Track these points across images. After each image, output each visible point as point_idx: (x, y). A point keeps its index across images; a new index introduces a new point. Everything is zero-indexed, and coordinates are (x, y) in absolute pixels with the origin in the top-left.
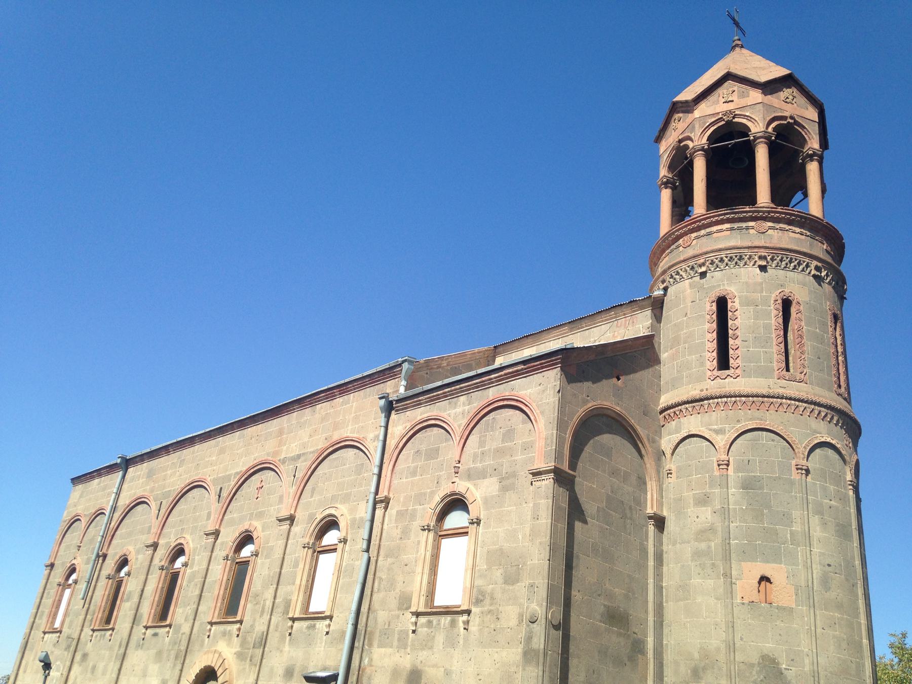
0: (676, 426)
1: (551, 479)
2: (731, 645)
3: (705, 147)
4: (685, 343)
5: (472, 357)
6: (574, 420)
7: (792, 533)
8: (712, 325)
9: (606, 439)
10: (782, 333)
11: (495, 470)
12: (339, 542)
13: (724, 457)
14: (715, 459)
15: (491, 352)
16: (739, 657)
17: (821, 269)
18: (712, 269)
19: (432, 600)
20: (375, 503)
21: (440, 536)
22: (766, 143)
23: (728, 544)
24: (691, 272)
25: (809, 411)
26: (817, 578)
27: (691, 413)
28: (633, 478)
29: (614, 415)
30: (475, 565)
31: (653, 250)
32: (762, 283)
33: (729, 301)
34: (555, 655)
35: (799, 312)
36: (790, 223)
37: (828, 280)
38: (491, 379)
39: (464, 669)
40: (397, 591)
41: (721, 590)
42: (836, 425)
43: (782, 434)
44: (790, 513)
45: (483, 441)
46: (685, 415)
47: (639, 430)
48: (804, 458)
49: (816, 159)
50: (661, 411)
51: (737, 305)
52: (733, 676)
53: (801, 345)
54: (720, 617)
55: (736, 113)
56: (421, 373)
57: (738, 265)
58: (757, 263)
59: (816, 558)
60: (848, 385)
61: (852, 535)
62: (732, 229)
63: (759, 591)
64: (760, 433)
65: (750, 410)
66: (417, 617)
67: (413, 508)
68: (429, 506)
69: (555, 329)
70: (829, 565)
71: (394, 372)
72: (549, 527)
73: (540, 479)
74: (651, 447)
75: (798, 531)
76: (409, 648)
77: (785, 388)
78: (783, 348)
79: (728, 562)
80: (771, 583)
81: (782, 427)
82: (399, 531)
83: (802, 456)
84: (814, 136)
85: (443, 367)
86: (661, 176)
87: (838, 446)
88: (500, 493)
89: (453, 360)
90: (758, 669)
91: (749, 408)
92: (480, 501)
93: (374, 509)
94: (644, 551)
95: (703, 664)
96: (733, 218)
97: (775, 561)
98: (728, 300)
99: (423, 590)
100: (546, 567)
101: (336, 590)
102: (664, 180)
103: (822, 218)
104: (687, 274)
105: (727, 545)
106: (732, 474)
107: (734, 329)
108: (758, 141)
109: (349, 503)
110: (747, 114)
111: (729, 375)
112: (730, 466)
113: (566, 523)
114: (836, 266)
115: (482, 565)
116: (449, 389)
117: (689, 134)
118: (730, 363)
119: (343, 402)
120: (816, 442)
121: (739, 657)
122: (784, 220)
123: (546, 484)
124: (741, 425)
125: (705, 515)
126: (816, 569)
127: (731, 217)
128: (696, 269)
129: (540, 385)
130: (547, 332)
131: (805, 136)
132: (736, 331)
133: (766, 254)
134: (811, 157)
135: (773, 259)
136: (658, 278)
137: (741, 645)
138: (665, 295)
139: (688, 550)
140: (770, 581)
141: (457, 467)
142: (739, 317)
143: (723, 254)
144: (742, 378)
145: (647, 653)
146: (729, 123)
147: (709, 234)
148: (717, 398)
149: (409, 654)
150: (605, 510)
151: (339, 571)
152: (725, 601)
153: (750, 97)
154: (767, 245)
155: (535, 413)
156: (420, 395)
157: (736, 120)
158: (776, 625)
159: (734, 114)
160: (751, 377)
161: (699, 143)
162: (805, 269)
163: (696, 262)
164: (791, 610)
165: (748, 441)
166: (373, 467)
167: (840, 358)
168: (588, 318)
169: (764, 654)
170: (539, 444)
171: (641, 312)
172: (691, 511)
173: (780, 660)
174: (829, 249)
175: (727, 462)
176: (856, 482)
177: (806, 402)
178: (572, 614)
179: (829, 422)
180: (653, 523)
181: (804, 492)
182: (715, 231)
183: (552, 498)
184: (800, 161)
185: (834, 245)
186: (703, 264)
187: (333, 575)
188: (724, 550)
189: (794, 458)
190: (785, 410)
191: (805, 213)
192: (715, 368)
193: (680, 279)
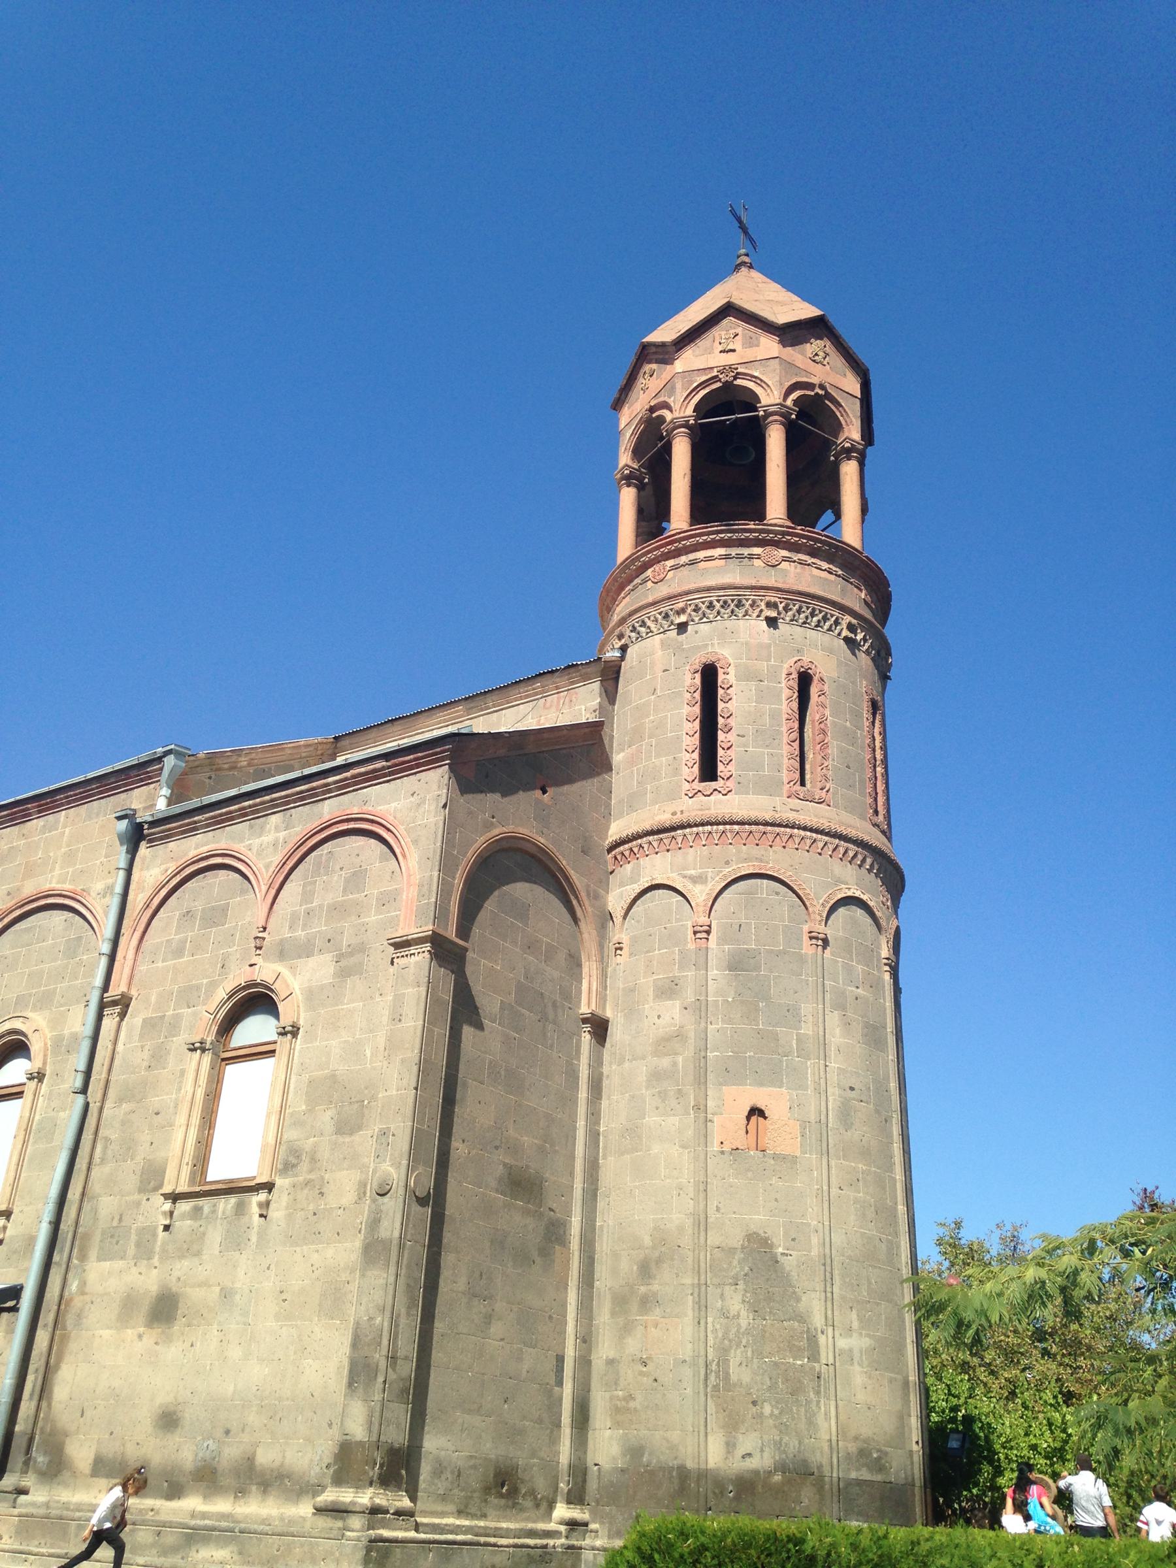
0: (632, 872)
1: (426, 953)
2: (701, 1220)
3: (690, 422)
4: (651, 738)
5: (295, 754)
6: (469, 854)
8: (694, 708)
9: (521, 890)
10: (796, 725)
11: (329, 941)
12: (28, 1079)
13: (703, 920)
14: (690, 924)
15: (328, 747)
16: (714, 1239)
17: (857, 630)
18: (696, 619)
19: (204, 1172)
20: (102, 1006)
21: (223, 1060)
22: (782, 423)
23: (704, 1057)
24: (665, 622)
25: (831, 849)
27: (657, 850)
28: (562, 956)
29: (533, 850)
30: (286, 1105)
31: (605, 585)
32: (770, 644)
33: (720, 671)
34: (419, 1248)
36: (813, 553)
37: (866, 647)
39: (256, 1285)
40: (139, 1158)
41: (690, 1132)
42: (870, 871)
43: (790, 883)
45: (310, 891)
46: (647, 853)
47: (574, 877)
49: (856, 457)
50: (610, 847)
51: (731, 678)
52: (702, 1270)
53: (824, 745)
55: (739, 370)
56: (198, 777)
58: (764, 613)
59: (833, 1077)
60: (888, 811)
61: (887, 1042)
62: (727, 557)
63: (747, 1132)
64: (759, 881)
65: (745, 844)
66: (174, 1202)
67: (176, 1012)
68: (205, 1008)
69: (442, 709)
70: (852, 1089)
71: (148, 772)
72: (419, 1033)
73: (406, 953)
74: (592, 906)
75: (807, 1035)
76: (157, 1257)
77: (798, 811)
78: (798, 749)
79: (703, 1088)
80: (765, 1118)
82: (146, 1055)
83: (819, 918)
84: (854, 420)
85: (241, 767)
86: (621, 464)
87: (871, 904)
88: (336, 980)
89: (260, 756)
90: (742, 1256)
92: (300, 998)
93: (100, 1017)
94: (573, 1075)
95: (657, 1254)
97: (772, 1083)
98: (719, 669)
99: (187, 1155)
100: (411, 1100)
101: (19, 1164)
102: (626, 472)
103: (859, 548)
104: (658, 626)
105: (702, 1060)
106: (715, 947)
107: (726, 716)
108: (771, 418)
109: (51, 1009)
110: (756, 374)
111: (715, 790)
112: (711, 934)
113: (448, 1028)
114: (878, 626)
115: (298, 1105)
116: (251, 802)
117: (666, 399)
118: (719, 771)
119: (44, 826)
120: (839, 896)
121: (714, 1239)
122: (804, 548)
123: (416, 963)
124: (730, 869)
125: (672, 1013)
126: (833, 1094)
127: (726, 538)
128: (672, 618)
129: (413, 795)
130: (426, 714)
131: (841, 418)
133: (777, 600)
134: (848, 453)
135: (786, 609)
136: (614, 629)
137: (717, 1218)
138: (622, 658)
139: (642, 1071)
140: (764, 1114)
141: (260, 938)
142: (734, 697)
143: (713, 596)
145: (570, 1243)
146: (728, 386)
147: (693, 563)
148: (696, 825)
149: (156, 1267)
151: (27, 1130)
152: (695, 1150)
153: (761, 347)
154: (780, 585)
155: (403, 843)
156: (196, 813)
157: (739, 382)
158: (771, 1185)
159: (735, 371)
161: (682, 415)
162: (833, 629)
163: (671, 607)
164: (794, 1160)
165: (740, 894)
166: (101, 943)
167: (879, 769)
168: (497, 692)
169: (749, 1232)
170: (407, 897)
172: (650, 1007)
174: (869, 599)
175: (708, 928)
176: (894, 960)
177: (828, 834)
178: (449, 1180)
179: (860, 866)
180: (589, 1029)
181: (820, 975)
182: (702, 558)
183: (426, 985)
184: (832, 458)
185: (877, 595)
186: (682, 611)
187: (15, 1138)
190: (796, 846)
191: (835, 539)
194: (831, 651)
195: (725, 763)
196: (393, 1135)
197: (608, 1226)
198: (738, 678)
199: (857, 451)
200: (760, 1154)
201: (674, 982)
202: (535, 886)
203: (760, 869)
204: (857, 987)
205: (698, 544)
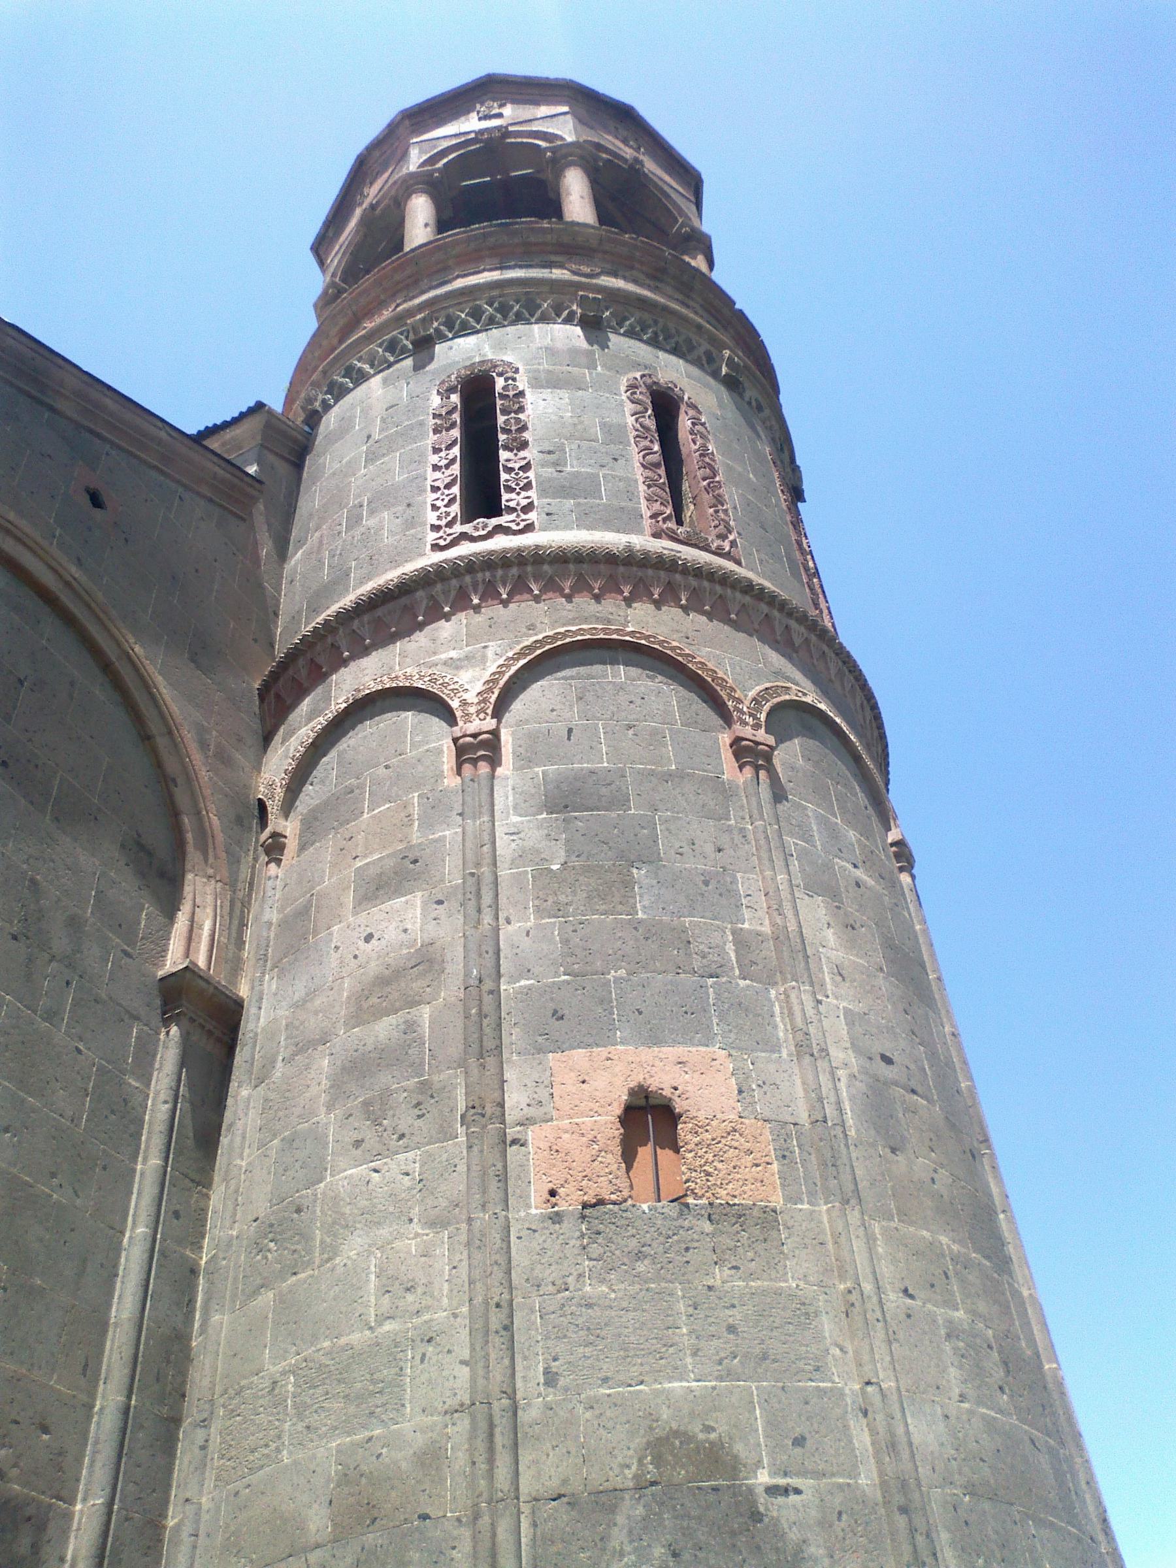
2: (497, 1421)
7: (742, 942)
23: (491, 992)
41: (456, 1184)
54: (445, 1301)
75: (758, 934)
105: (488, 999)
124: (540, 637)
158: (710, 1288)
164: (769, 1218)
173: (739, 1448)
197: (198, 1514)
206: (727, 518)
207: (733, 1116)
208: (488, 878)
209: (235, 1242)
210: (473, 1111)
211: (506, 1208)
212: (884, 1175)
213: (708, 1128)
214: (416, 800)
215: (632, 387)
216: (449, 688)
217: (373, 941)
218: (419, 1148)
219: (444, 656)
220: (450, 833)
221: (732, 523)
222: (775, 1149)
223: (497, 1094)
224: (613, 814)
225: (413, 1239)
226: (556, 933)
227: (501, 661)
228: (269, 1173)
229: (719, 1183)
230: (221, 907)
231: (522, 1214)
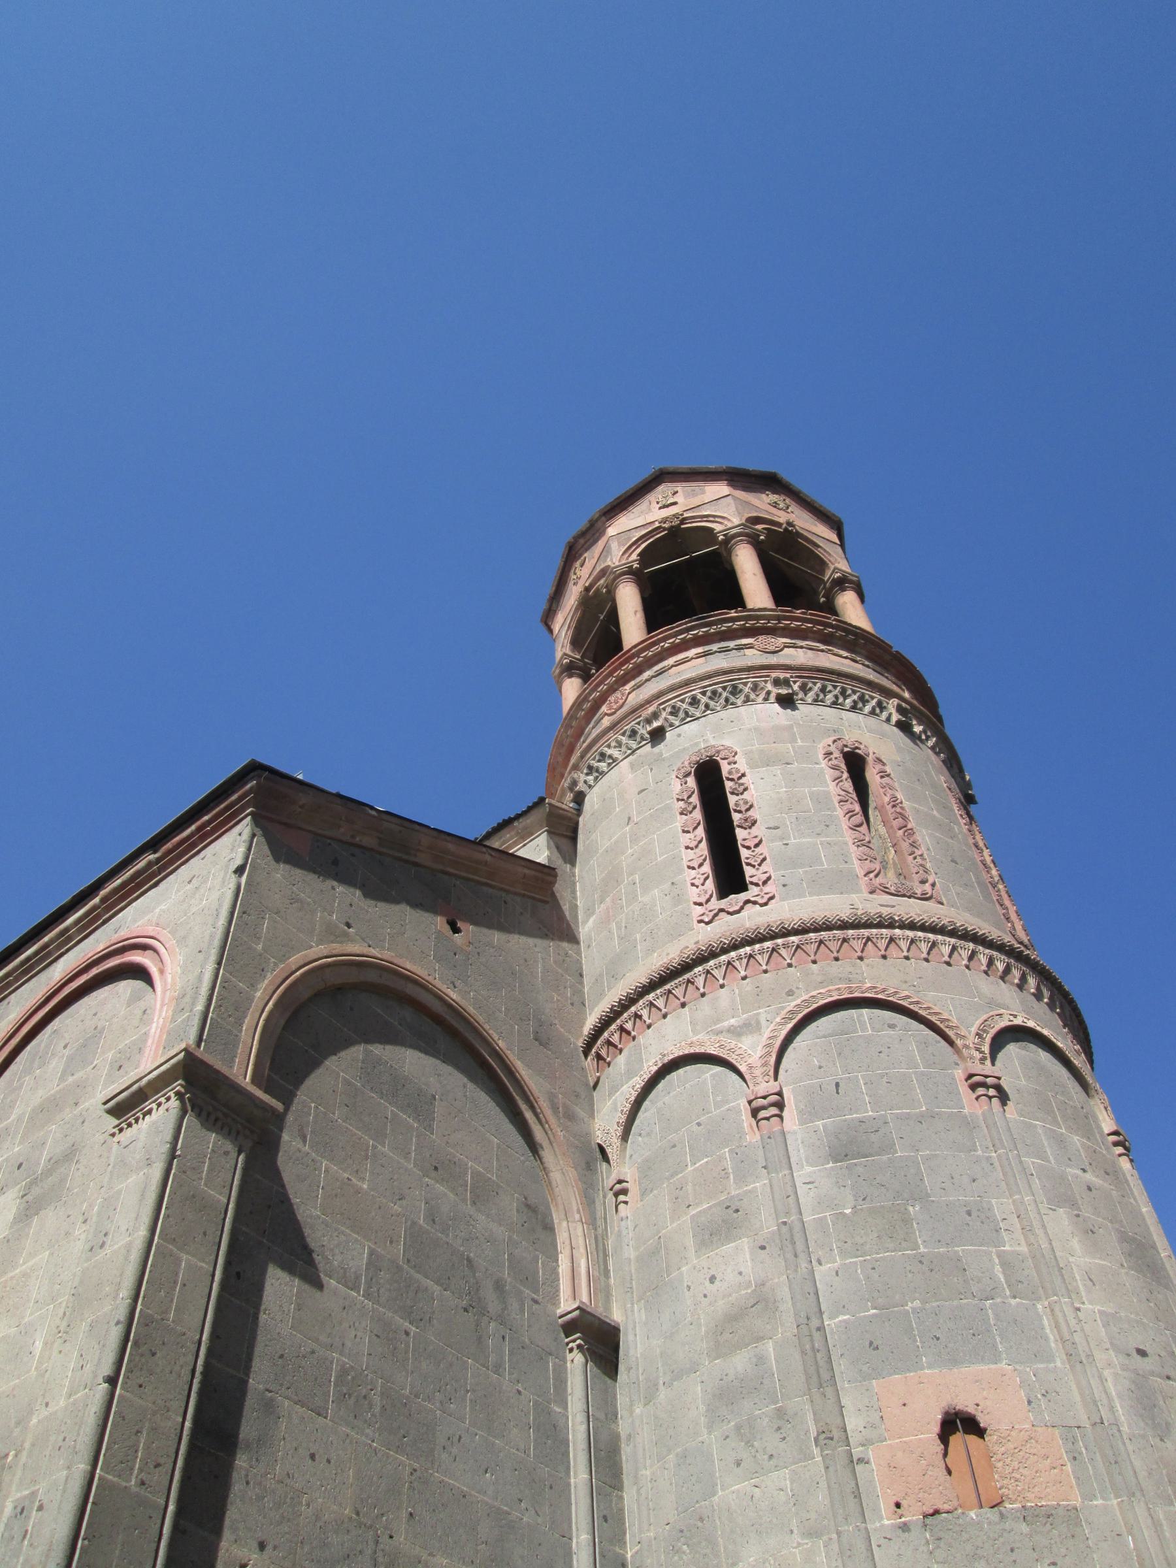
1: (173, 1099)
7: (1005, 1264)
13: (766, 1086)
14: (743, 1103)
22: (749, 543)
23: (818, 1329)
26: (1119, 1396)
27: (664, 1010)
28: (509, 1203)
29: (437, 1007)
32: (791, 727)
35: (884, 775)
38: (67, 930)
41: (821, 1498)
44: (985, 1205)
46: (648, 1022)
47: (523, 1073)
48: (983, 1060)
49: (852, 587)
51: (742, 765)
53: (910, 833)
55: (686, 515)
57: (732, 704)
64: (853, 1013)
65: (814, 962)
70: (1142, 1353)
72: (135, 1256)
74: (565, 1128)
79: (829, 1391)
80: (980, 1432)
81: (906, 993)
83: (978, 1055)
91: (813, 957)
96: (706, 634)
105: (817, 1336)
107: (743, 809)
111: (747, 902)
122: (810, 635)
124: (798, 1001)
127: (701, 633)
132: (749, 813)
134: (842, 583)
135: (804, 688)
138: (579, 812)
139: (696, 1392)
142: (752, 786)
144: (783, 899)
148: (725, 951)
150: (399, 1269)
152: (839, 1533)
153: (707, 494)
160: (805, 896)
162: (878, 710)
163: (638, 720)
165: (825, 1037)
171: (524, 845)
175: (776, 1097)
177: (953, 933)
180: (579, 1342)
186: (655, 716)
188: (809, 1352)
189: (957, 1064)
190: (905, 954)
192: (711, 896)
193: (609, 764)
194: (883, 735)
195: (756, 864)
196: (40, 1508)
198: (753, 765)
199: (851, 582)
200: (993, 1515)
201: (733, 1208)
202: (447, 1069)
203: (851, 993)
204: (1084, 1170)
205: (664, 650)
206: (923, 863)
207: (1027, 1426)
208: (797, 1227)
209: (653, 1542)
210: (824, 1436)
211: (864, 1521)
212: (1157, 1463)
213: (1009, 1438)
214: (727, 1154)
215: (828, 754)
216: (736, 1053)
217: (717, 1282)
218: (786, 1467)
219: (726, 1024)
220: (760, 1184)
221: (928, 865)
222: (1066, 1452)
223: (839, 1421)
224: (885, 1158)
225: (796, 1548)
226: (859, 1271)
227: (772, 1027)
228: (671, 1484)
229: (1026, 1488)
230: (590, 1245)
231: (878, 1525)
